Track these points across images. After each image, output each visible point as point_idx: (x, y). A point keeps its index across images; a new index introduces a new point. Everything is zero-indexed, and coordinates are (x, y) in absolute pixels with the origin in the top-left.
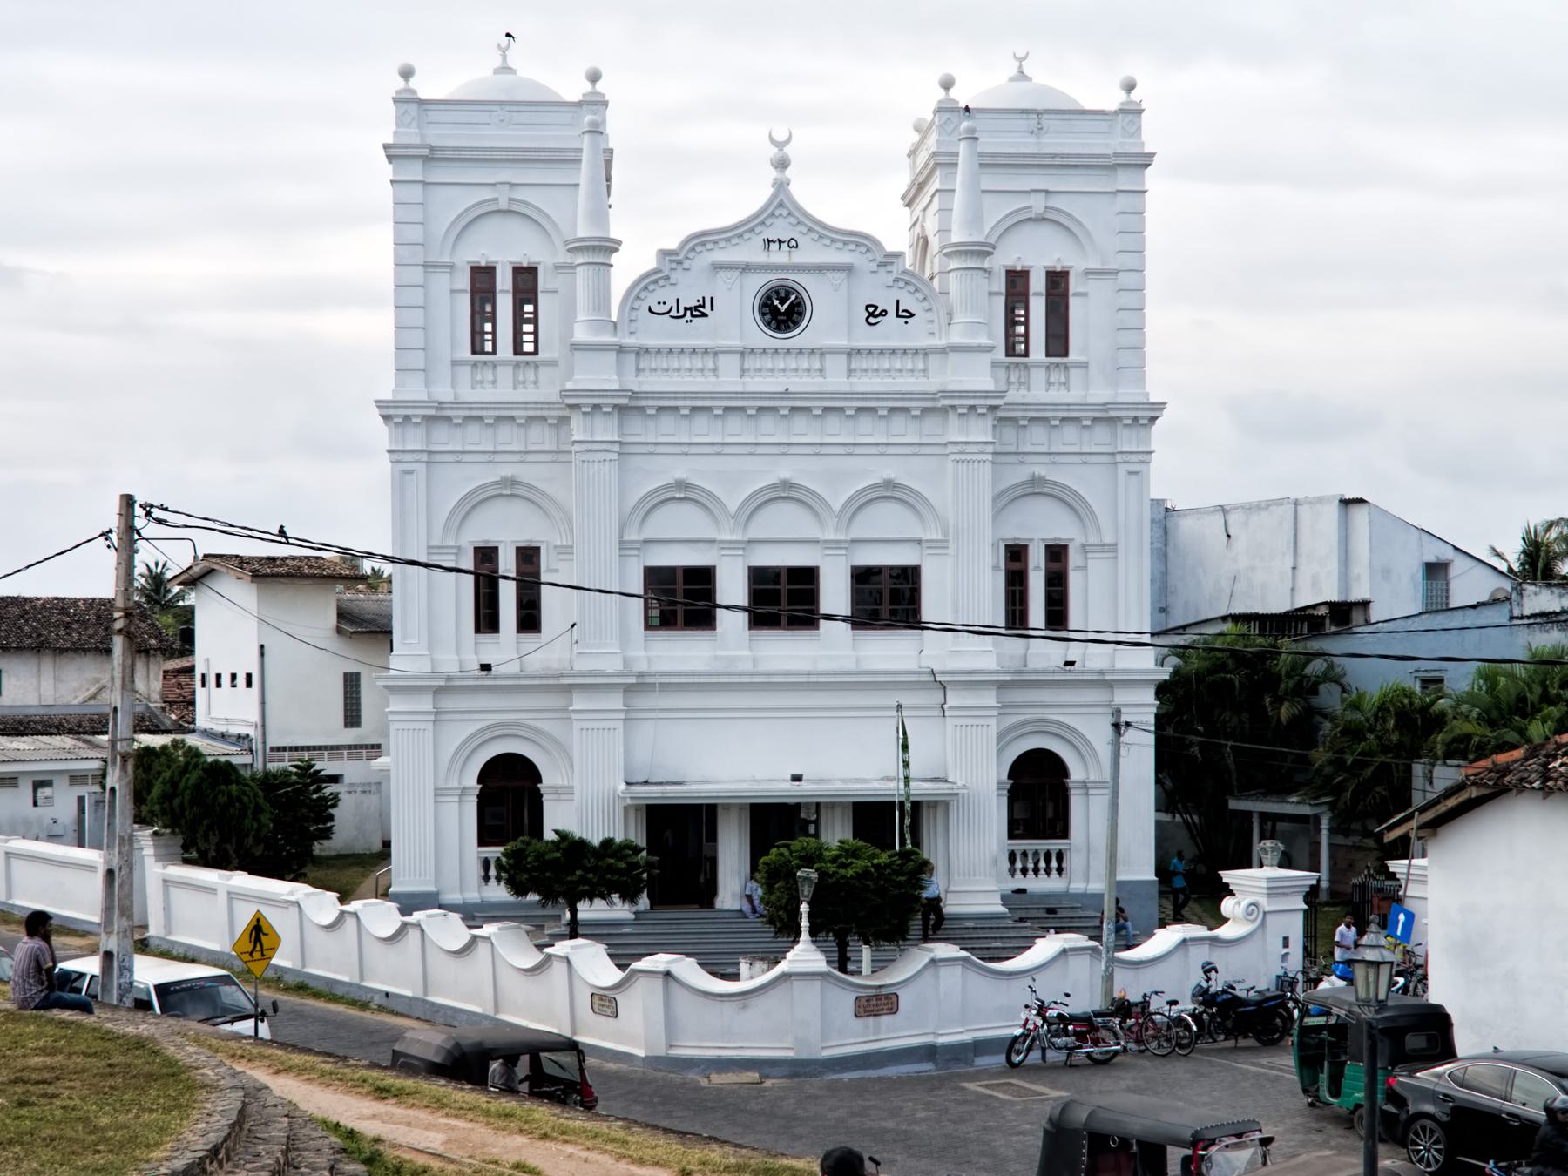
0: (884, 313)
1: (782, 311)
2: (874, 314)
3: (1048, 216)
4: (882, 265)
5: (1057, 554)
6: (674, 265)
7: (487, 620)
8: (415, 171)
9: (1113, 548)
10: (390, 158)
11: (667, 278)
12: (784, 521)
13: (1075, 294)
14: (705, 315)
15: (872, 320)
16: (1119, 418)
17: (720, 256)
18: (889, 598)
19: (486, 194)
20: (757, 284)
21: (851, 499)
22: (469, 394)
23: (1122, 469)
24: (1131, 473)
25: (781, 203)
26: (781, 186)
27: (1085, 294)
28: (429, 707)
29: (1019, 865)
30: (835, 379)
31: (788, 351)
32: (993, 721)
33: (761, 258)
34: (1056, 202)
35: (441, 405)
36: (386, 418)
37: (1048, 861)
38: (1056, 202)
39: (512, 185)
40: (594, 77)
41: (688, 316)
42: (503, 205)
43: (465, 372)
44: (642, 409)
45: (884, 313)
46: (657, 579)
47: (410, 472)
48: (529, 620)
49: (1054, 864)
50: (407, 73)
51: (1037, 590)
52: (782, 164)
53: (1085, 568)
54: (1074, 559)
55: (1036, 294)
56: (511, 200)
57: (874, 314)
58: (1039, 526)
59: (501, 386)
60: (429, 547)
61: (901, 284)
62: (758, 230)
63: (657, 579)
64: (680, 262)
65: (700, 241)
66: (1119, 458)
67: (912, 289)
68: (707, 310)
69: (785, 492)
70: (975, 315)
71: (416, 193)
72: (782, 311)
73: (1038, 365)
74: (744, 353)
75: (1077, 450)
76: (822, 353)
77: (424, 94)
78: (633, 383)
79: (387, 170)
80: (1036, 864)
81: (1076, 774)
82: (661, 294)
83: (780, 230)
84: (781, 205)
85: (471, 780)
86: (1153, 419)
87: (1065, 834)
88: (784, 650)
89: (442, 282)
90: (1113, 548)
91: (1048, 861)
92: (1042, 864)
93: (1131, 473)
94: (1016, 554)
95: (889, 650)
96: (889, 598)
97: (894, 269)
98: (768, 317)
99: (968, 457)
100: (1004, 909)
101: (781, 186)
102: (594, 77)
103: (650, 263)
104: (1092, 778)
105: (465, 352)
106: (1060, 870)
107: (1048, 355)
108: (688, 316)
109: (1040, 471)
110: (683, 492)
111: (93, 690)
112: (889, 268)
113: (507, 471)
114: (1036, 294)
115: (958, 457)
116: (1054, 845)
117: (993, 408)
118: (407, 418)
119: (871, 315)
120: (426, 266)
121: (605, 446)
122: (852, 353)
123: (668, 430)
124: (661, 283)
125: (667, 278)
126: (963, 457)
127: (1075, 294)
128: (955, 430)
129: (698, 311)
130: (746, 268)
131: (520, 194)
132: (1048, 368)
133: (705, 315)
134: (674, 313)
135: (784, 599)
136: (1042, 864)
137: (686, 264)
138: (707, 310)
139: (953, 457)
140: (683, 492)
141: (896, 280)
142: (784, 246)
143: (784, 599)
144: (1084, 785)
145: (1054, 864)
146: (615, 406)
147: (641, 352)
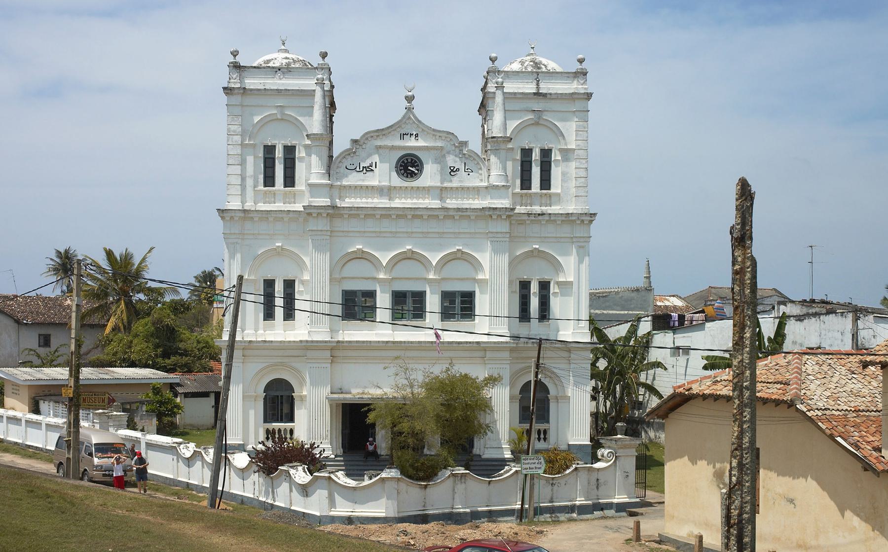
0: (458, 170)
1: (409, 166)
2: (453, 171)
8: (236, 99)
10: (226, 94)
11: (355, 153)
12: (408, 269)
22: (262, 207)
26: (409, 109)
32: (508, 366)
33: (398, 143)
36: (223, 218)
40: (324, 55)
44: (342, 215)
45: (458, 170)
49: (542, 436)
50: (235, 54)
52: (410, 99)
57: (453, 171)
65: (370, 135)
66: (574, 240)
70: (499, 171)
71: (237, 110)
75: (554, 235)
79: (224, 98)
84: (410, 118)
86: (591, 221)
87: (548, 422)
101: (409, 109)
102: (324, 55)
103: (347, 145)
106: (545, 439)
117: (509, 217)
118: (232, 218)
119: (452, 171)
122: (442, 189)
123: (354, 225)
125: (355, 153)
130: (393, 148)
135: (409, 305)
140: (361, 256)
144: (557, 398)
145: (542, 436)
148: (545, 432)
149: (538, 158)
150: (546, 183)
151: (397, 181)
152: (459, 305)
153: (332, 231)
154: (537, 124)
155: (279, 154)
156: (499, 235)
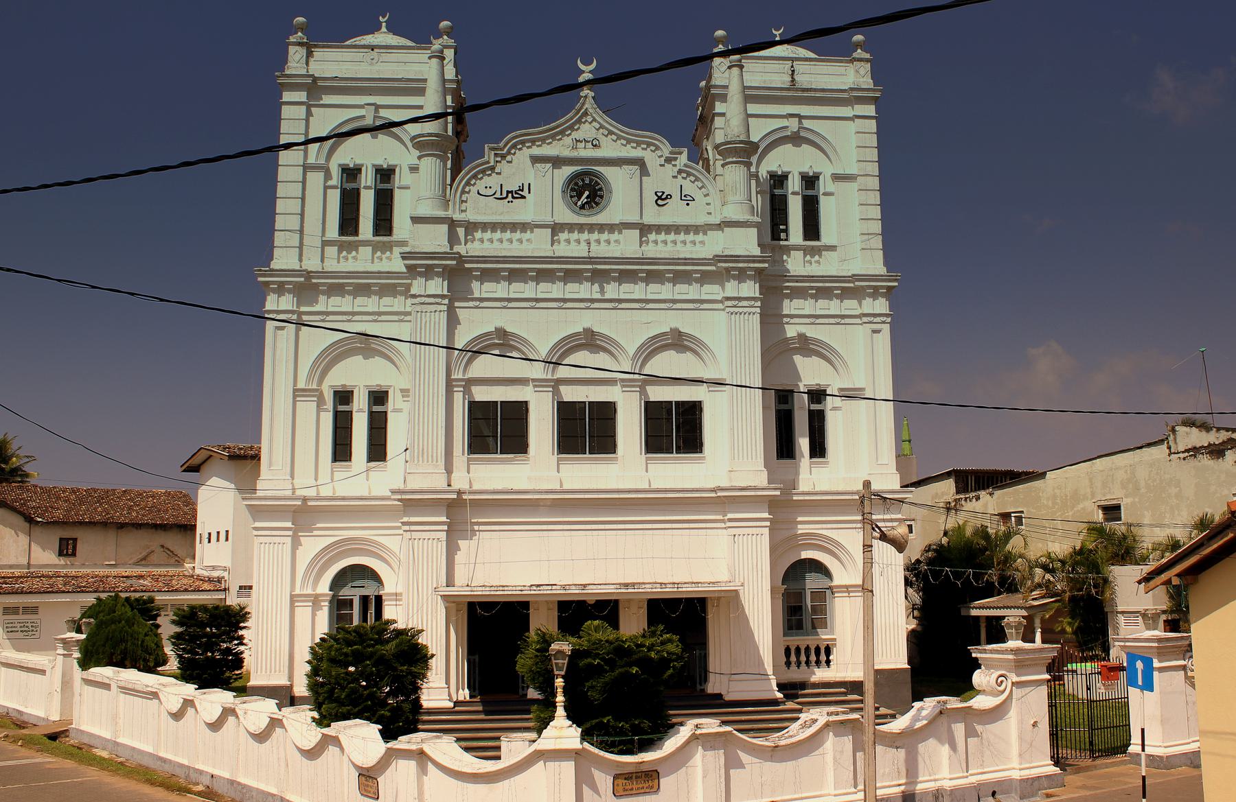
3: (802, 134)
7: (342, 451)
14: (523, 197)
15: (660, 202)
17: (536, 151)
20: (568, 171)
21: (643, 345)
24: (874, 331)
32: (766, 531)
33: (567, 153)
34: (807, 123)
35: (308, 275)
38: (807, 123)
43: (332, 251)
46: (480, 414)
47: (282, 328)
48: (377, 451)
57: (662, 198)
59: (362, 261)
60: (295, 391)
63: (480, 414)
67: (693, 178)
68: (525, 193)
69: (590, 341)
74: (556, 228)
78: (461, 249)
82: (487, 181)
85: (324, 587)
88: (586, 474)
89: (315, 179)
93: (874, 331)
95: (674, 473)
96: (676, 429)
97: (677, 163)
99: (741, 310)
105: (333, 232)
111: (144, 554)
114: (794, 193)
115: (732, 310)
119: (660, 198)
122: (645, 230)
125: (492, 168)
126: (736, 310)
128: (731, 288)
129: (518, 194)
130: (557, 162)
133: (523, 197)
134: (498, 195)
135: (585, 430)
137: (509, 158)
138: (525, 193)
139: (728, 310)
141: (680, 172)
147: (471, 227)
148: (828, 651)
149: (797, 188)
150: (812, 228)
151: (565, 215)
152: (676, 429)
155: (367, 178)
156: (745, 303)
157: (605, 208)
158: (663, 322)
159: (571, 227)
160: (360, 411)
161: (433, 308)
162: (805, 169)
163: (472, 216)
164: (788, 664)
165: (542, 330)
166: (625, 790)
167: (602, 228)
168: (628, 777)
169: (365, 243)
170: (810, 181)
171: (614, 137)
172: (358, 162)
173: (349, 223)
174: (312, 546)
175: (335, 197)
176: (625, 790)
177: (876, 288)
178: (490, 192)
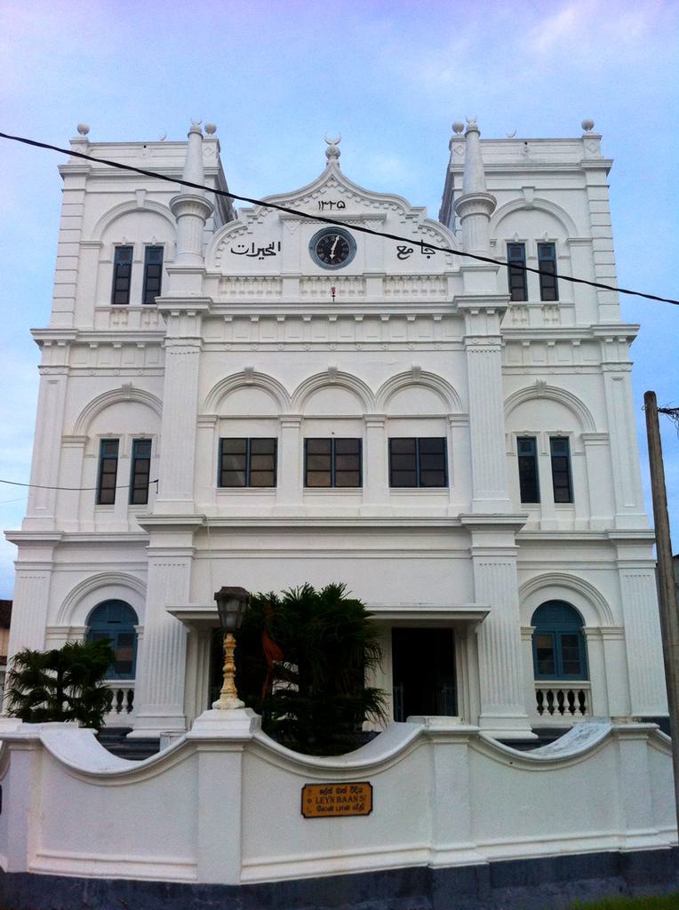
1: (333, 247)
3: (536, 205)
4: (409, 217)
5: (560, 444)
6: (251, 220)
9: (605, 437)
13: (560, 258)
15: (401, 256)
16: (602, 338)
18: (421, 463)
19: (131, 198)
23: (608, 376)
25: (332, 177)
27: (568, 258)
28: (49, 559)
29: (546, 703)
30: (375, 293)
31: (337, 278)
35: (79, 334)
36: (40, 343)
37: (571, 700)
39: (148, 192)
41: (261, 255)
42: (140, 205)
49: (577, 703)
51: (544, 469)
52: (333, 154)
53: (584, 454)
54: (574, 447)
55: (531, 258)
56: (145, 201)
58: (544, 422)
60: (63, 437)
61: (424, 230)
62: (315, 195)
64: (255, 218)
66: (605, 368)
68: (275, 250)
69: (333, 380)
72: (333, 247)
73: (535, 306)
74: (303, 279)
75: (570, 364)
76: (362, 278)
77: (91, 141)
80: (561, 702)
81: (590, 622)
82: (240, 240)
83: (332, 194)
89: (91, 255)
90: (605, 437)
91: (571, 700)
92: (567, 703)
94: (526, 445)
98: (322, 255)
100: (535, 736)
104: (605, 625)
105: (105, 299)
106: (583, 709)
107: (542, 300)
108: (261, 255)
109: (543, 379)
110: (250, 380)
112: (415, 219)
113: (127, 381)
116: (575, 684)
118: (55, 343)
119: (402, 252)
120: (82, 244)
121: (190, 342)
122: (387, 278)
124: (241, 232)
127: (560, 258)
129: (268, 252)
131: (152, 198)
132: (543, 309)
134: (250, 253)
135: (334, 463)
136: (567, 703)
137: (260, 220)
142: (334, 206)
143: (334, 463)
144: (599, 632)
145: (577, 703)
146: (199, 312)
147: (223, 279)
151: (315, 269)
152: (421, 463)
153: (204, 343)
154: (530, 209)
155: (139, 255)
157: (350, 261)
158: (406, 362)
159: (319, 278)
160: (124, 456)
161: (186, 349)
162: (541, 236)
163: (226, 272)
164: (541, 709)
165: (290, 371)
166: (320, 809)
167: (347, 278)
168: (326, 789)
169: (135, 309)
170: (547, 248)
171: (358, 199)
172: (130, 240)
173: (120, 293)
174: (68, 582)
175: (108, 272)
176: (320, 809)
177: (616, 338)
178: (243, 250)
